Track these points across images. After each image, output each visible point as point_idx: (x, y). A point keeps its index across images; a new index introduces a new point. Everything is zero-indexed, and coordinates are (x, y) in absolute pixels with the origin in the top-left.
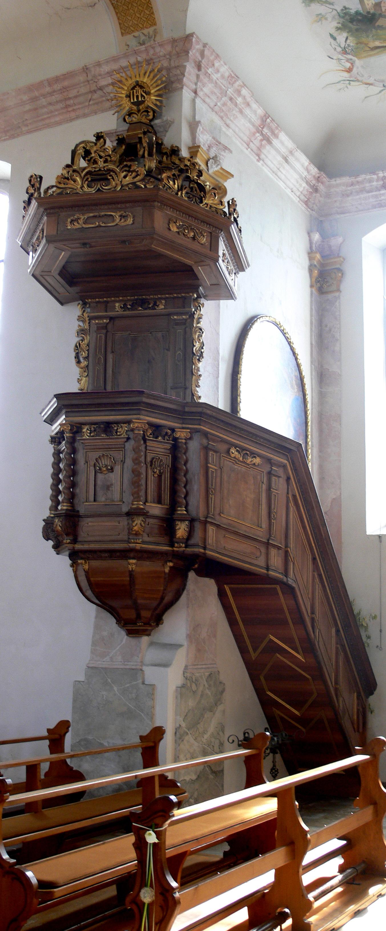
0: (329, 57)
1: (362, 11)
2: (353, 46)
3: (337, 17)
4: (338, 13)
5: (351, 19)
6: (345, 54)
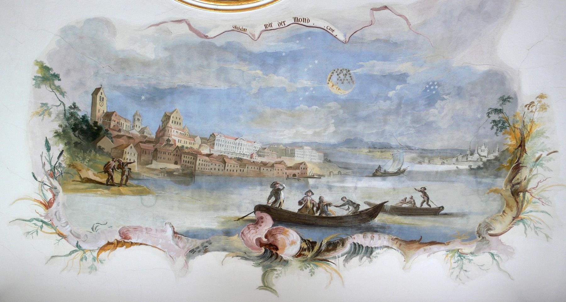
0: (34, 176)
1: (89, 119)
2: (64, 168)
3: (62, 116)
4: (65, 110)
5: (75, 125)
6: (52, 177)
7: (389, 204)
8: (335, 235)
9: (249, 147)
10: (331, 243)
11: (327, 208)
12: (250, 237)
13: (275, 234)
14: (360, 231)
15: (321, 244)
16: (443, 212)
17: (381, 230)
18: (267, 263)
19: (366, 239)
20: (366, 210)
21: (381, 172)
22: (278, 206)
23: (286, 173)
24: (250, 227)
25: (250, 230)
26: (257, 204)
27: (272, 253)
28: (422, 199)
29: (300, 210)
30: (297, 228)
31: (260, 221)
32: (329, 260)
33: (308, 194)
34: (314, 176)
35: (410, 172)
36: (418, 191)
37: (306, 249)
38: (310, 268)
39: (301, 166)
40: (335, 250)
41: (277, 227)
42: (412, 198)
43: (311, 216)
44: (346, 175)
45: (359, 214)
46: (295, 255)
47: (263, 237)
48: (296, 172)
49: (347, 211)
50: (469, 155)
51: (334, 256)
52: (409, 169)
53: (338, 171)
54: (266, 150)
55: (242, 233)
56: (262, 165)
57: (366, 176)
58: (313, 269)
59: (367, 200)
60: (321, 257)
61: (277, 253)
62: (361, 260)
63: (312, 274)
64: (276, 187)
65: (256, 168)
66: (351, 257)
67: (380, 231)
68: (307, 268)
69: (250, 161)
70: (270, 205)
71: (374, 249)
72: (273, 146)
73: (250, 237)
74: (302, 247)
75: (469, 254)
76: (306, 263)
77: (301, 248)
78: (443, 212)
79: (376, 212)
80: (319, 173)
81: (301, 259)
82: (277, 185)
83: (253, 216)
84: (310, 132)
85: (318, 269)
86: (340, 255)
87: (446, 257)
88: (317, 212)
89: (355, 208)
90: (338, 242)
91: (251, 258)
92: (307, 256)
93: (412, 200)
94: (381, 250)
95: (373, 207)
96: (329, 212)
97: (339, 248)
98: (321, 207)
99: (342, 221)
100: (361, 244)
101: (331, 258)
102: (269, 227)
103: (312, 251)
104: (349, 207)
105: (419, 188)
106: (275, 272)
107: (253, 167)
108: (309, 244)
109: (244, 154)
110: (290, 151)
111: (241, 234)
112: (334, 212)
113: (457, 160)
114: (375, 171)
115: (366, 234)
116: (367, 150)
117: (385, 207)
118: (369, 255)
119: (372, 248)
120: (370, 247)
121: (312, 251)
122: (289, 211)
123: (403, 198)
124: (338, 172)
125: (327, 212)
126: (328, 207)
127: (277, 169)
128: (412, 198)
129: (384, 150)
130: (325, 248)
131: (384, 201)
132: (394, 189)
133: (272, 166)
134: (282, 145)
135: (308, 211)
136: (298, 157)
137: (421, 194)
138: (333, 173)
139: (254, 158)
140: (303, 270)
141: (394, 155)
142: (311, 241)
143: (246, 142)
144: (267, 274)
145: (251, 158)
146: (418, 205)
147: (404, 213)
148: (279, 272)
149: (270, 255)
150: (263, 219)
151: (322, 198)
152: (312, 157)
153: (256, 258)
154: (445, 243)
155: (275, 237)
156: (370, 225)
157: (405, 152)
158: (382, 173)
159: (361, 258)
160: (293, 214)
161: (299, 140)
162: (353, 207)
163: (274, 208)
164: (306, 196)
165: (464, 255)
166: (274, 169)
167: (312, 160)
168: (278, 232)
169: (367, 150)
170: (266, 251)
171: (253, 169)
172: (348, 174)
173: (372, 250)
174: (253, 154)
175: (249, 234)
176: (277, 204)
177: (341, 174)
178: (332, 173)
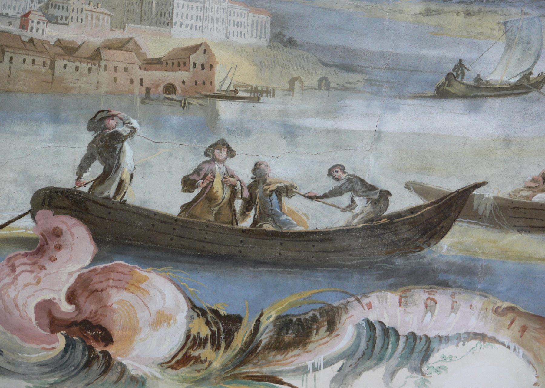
8: (305, 296)
10: (291, 320)
11: (280, 201)
12: (16, 297)
13: (102, 290)
15: (258, 322)
17: (461, 280)
19: (408, 310)
20: (412, 211)
21: (463, 84)
23: (141, 80)
24: (17, 262)
25: (17, 273)
26: (42, 184)
27: (90, 354)
29: (186, 207)
30: (177, 268)
31: (51, 244)
32: (285, 380)
33: (216, 152)
34: (236, 91)
37: (206, 339)
40: (305, 344)
41: (108, 265)
44: (345, 89)
45: (387, 224)
46: (170, 362)
47: (60, 299)
51: (300, 365)
53: (317, 78)
56: (59, 50)
57: (415, 97)
59: (414, 177)
60: (257, 369)
61: (106, 354)
62: (392, 379)
64: (105, 128)
66: (358, 370)
67: (455, 282)
69: (21, 38)
70: (85, 189)
71: (434, 345)
73: (16, 297)
74: (194, 332)
77: (188, 337)
79: (446, 218)
80: (254, 83)
81: (187, 375)
82: (112, 123)
86: (320, 359)
88: (245, 213)
89: (375, 203)
90: (314, 319)
91: (20, 370)
92: (210, 363)
94: (457, 346)
95: (434, 200)
96: (284, 217)
98: (260, 199)
99: (328, 246)
100: (392, 325)
101: (288, 371)
102: (81, 265)
103: (227, 347)
104: (353, 201)
107: (29, 59)
108: (216, 324)
112: (304, 218)
114: (443, 79)
115: (408, 294)
116: (419, 8)
117: (475, 203)
118: (417, 363)
119: (428, 339)
120: (421, 338)
121: (227, 347)
122: (149, 211)
124: (320, 81)
125: (278, 216)
126: (284, 200)
127: (111, 65)
130: (271, 337)
131: (472, 182)
132: (507, 142)
135: (214, 212)
136: (184, 26)
138: (301, 82)
139: (32, 28)
141: (509, 26)
142: (223, 312)
145: (24, 26)
147: (538, 223)
149: (85, 358)
150: (62, 238)
151: (262, 166)
152: (231, 29)
153: (36, 368)
155: (100, 300)
156: (425, 261)
158: (468, 86)
159: (393, 374)
160: (162, 222)
162: (369, 199)
163: (100, 201)
164: (208, 159)
166: (99, 66)
167: (231, 38)
168: (111, 282)
169: (419, 8)
170: (70, 346)
171: (28, 66)
172: (352, 86)
173: (428, 348)
174: (30, 12)
175: (13, 287)
176: (110, 186)
177: (328, 87)
178: (297, 84)
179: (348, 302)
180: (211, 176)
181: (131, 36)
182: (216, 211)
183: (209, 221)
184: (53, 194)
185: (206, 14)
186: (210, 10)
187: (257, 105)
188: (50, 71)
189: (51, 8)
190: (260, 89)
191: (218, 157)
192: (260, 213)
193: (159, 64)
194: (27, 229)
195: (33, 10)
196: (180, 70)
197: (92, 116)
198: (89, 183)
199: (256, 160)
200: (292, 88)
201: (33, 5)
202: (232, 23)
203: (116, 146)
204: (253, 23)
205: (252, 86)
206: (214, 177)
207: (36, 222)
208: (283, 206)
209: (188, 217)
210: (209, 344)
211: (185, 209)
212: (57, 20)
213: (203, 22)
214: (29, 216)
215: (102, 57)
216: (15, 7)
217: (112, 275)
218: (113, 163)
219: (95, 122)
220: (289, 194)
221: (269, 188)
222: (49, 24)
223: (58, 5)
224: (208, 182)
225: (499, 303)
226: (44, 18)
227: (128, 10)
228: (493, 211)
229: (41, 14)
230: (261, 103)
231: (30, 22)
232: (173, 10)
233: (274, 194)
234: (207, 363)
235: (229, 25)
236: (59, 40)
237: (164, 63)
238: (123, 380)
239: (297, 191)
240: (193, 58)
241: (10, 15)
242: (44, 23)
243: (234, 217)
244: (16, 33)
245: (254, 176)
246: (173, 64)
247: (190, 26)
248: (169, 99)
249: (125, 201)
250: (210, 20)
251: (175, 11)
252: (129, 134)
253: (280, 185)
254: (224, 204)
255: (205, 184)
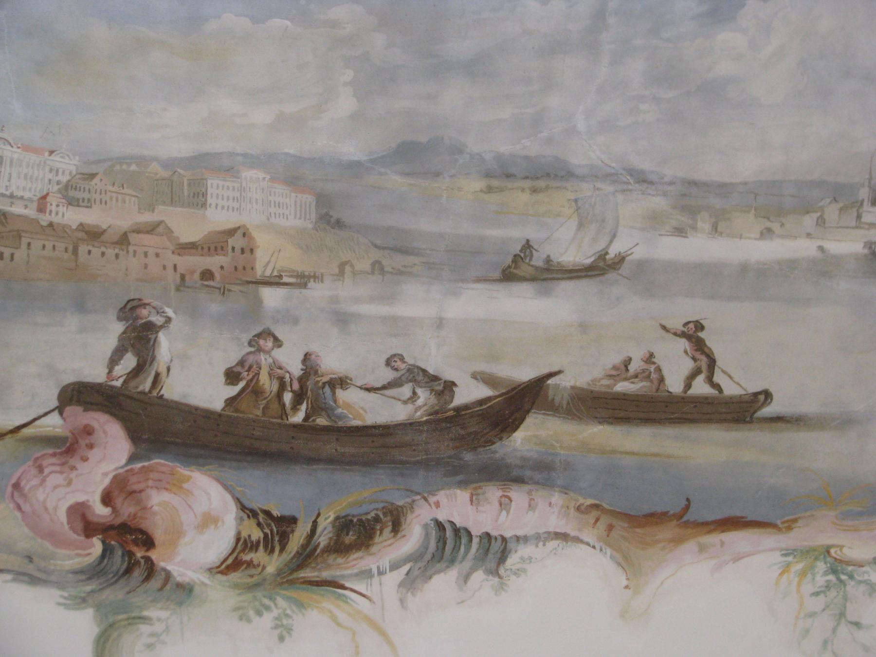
7: (565, 382)
9: (32, 168)
10: (351, 521)
11: (334, 393)
12: (45, 500)
13: (141, 491)
14: (460, 477)
15: (315, 524)
16: (768, 411)
17: (537, 476)
18: (115, 594)
19: (480, 508)
20: (481, 402)
21: (532, 266)
22: (147, 385)
23: (175, 267)
24: (45, 463)
25: (45, 474)
26: (70, 379)
27: (130, 559)
28: (688, 365)
29: (230, 402)
30: (223, 466)
31: (83, 443)
32: (347, 585)
33: (262, 342)
34: (280, 277)
35: (643, 266)
36: (675, 334)
37: (258, 542)
38: (275, 612)
39: (230, 241)
40: (368, 546)
41: (146, 464)
42: (650, 358)
43: (273, 424)
44: (400, 273)
45: (453, 417)
46: (218, 567)
47: (94, 502)
48: (213, 262)
49: (410, 407)
50: (865, 203)
51: (364, 568)
52: (639, 253)
54: (96, 180)
55: (17, 486)
56: (82, 235)
57: (479, 280)
58: (287, 616)
59: (482, 367)
60: (316, 574)
61: (148, 560)
62: (466, 582)
63: (285, 633)
65: (61, 246)
66: (429, 573)
68: (265, 613)
69: (39, 223)
70: (118, 383)
71: (511, 545)
72: (124, 167)
73: (45, 500)
74: (244, 535)
75: (869, 563)
76: (259, 594)
77: (238, 540)
78: (768, 411)
80: (299, 268)
81: (239, 580)
82: (144, 312)
83: (54, 424)
84: (262, 116)
85: (303, 615)
86: (385, 562)
87: (782, 574)
88: (295, 407)
89: (439, 394)
90: (377, 519)
91: (53, 578)
92: (264, 568)
93: (652, 368)
94: (537, 546)
95: (504, 391)
96: (340, 410)
97: (382, 539)
98: (312, 391)
99: (390, 440)
100: (464, 525)
101: (351, 576)
103: (282, 550)
104: (414, 393)
105: (677, 325)
106: (144, 628)
107: (49, 245)
108: (269, 525)
109: (12, 196)
110: (189, 185)
111: (9, 489)
112: (361, 411)
113: (821, 222)
114: (509, 260)
115: (479, 491)
116: (478, 185)
117: (551, 393)
118: (493, 565)
119: (504, 539)
120: (496, 538)
121: (282, 550)
123: (617, 359)
124: (373, 265)
125: (333, 409)
128: (650, 358)
129: (541, 184)
130: (330, 539)
131: (545, 371)
132: (584, 327)
133: (123, 240)
134: (155, 163)
135: (262, 406)
136: (219, 208)
137: (684, 343)
138: (352, 266)
139: (51, 212)
140: (249, 621)
141: (580, 203)
142: (276, 513)
143: (19, 150)
144: (115, 634)
145: (41, 209)
146: (675, 384)
147: (622, 414)
148: (158, 627)
149: (126, 564)
151: (313, 357)
152: (272, 210)
153: (70, 575)
154: (779, 522)
155: (139, 502)
156: (497, 455)
157: (623, 191)
158: (537, 268)
159: (466, 578)
160: (204, 417)
161: (220, 144)
162: (432, 390)
163: (135, 396)
164: (252, 349)
165: (850, 568)
166: (128, 252)
167: (273, 220)
168: (150, 483)
169: (478, 185)
170: (107, 551)
171: (48, 252)
172: (408, 269)
173: (505, 548)
174: (48, 194)
175: (41, 490)
176: (145, 379)
177: (382, 271)
178: (348, 268)
179: (414, 501)
180: (257, 367)
181: (162, 219)
182: (264, 405)
183: (257, 416)
184: (81, 388)
185: (243, 194)
186: (248, 190)
187: (304, 291)
188: (73, 257)
189: (71, 190)
190: (307, 274)
191: (263, 347)
192: (312, 407)
193: (194, 248)
194: (54, 427)
195: (52, 192)
196: (217, 254)
197: (123, 305)
198: (121, 376)
199: (306, 350)
200: (342, 273)
201: (50, 186)
202: (273, 203)
203: (150, 336)
204: (295, 205)
205: (298, 272)
206: (260, 368)
207: (64, 419)
208: (337, 399)
209: (233, 412)
210: (261, 548)
211: (230, 403)
212: (78, 203)
213: (240, 203)
214: (56, 413)
215: (131, 241)
216: (30, 189)
217: (152, 475)
218: (148, 355)
219: (126, 312)
220: (343, 386)
221: (321, 380)
222: (70, 207)
223: (78, 186)
224: (254, 374)
225: (581, 501)
226: (64, 201)
227: (157, 192)
228: (570, 401)
229: (60, 196)
230: (308, 289)
231: (49, 204)
232: (206, 191)
233: (327, 386)
234: (260, 569)
235: (270, 206)
236: (81, 224)
237: (200, 248)
238: (168, 587)
239: (353, 383)
240: (231, 242)
241: (26, 197)
242: (64, 206)
243: (283, 411)
244: (34, 217)
245: (304, 368)
246: (209, 248)
247: (226, 208)
248: (207, 286)
249: (162, 395)
250: (248, 201)
251: (210, 191)
252: (164, 324)
253: (334, 376)
254: (272, 398)
255: (251, 376)
